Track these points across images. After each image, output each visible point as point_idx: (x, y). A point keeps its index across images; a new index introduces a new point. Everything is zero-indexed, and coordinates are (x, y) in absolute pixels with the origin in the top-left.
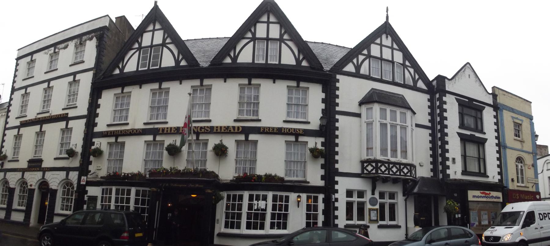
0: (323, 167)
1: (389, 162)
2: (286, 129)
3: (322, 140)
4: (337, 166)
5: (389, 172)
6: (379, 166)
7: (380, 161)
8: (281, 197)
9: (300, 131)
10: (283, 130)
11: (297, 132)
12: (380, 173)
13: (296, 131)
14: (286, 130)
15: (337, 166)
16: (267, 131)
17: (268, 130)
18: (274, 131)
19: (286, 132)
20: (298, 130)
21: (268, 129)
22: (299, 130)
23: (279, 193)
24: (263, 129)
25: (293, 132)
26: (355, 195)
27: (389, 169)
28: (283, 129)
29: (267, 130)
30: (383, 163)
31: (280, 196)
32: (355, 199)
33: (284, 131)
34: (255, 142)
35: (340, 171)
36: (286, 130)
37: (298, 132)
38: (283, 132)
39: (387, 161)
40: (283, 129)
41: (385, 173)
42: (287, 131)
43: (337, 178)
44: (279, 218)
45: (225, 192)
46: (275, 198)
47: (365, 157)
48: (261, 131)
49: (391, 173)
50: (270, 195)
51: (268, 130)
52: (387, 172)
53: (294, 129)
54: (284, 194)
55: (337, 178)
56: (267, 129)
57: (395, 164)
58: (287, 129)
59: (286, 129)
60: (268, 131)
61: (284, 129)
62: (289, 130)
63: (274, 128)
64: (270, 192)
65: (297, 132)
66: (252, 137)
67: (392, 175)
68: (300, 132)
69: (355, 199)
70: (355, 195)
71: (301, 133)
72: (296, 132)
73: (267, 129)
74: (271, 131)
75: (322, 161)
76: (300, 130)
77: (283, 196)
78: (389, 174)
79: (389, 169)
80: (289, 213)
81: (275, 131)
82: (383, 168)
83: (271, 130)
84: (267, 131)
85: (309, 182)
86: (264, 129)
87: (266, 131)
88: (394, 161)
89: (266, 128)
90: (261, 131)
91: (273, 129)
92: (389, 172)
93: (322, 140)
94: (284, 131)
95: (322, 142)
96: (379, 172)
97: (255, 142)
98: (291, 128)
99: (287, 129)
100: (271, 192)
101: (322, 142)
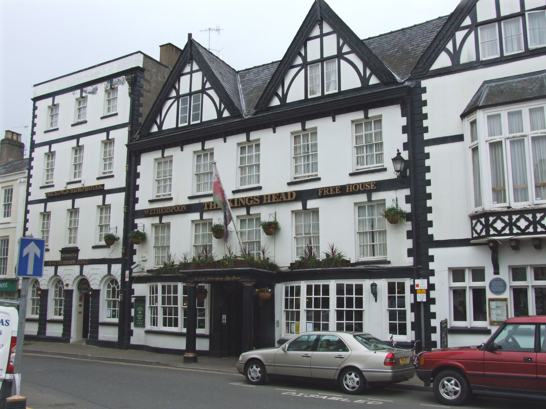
0: (409, 235)
1: (510, 212)
2: (351, 186)
3: (407, 192)
4: (430, 231)
5: (511, 230)
6: (490, 222)
7: (492, 214)
8: (349, 287)
9: (370, 185)
10: (347, 188)
11: (366, 189)
12: (494, 235)
13: (365, 186)
14: (351, 188)
15: (430, 231)
16: (326, 193)
17: (328, 192)
18: (335, 192)
19: (351, 191)
20: (368, 184)
21: (328, 190)
22: (369, 183)
23: (346, 282)
24: (321, 192)
25: (361, 189)
26: (468, 276)
27: (511, 224)
28: (347, 186)
29: (327, 192)
30: (498, 215)
31: (347, 285)
32: (468, 283)
33: (349, 190)
34: (316, 211)
35: (436, 238)
36: (351, 188)
37: (368, 188)
38: (347, 191)
39: (505, 209)
40: (347, 186)
41: (503, 233)
42: (352, 190)
43: (432, 252)
44: (349, 318)
45: (282, 283)
46: (340, 290)
47: (473, 209)
48: (320, 194)
49: (515, 231)
50: (333, 284)
51: (328, 192)
52: (507, 231)
53: (362, 184)
54: (354, 282)
55: (432, 252)
56: (326, 190)
57: (522, 213)
58: (352, 186)
59: (351, 186)
60: (328, 193)
61: (349, 187)
62: (356, 187)
63: (335, 187)
64: (332, 280)
65: (366, 189)
66: (311, 204)
67: (517, 234)
68: (370, 188)
69: (468, 283)
70: (468, 276)
71: (372, 188)
72: (365, 188)
73: (326, 190)
74: (331, 193)
75: (408, 226)
76: (370, 184)
77: (353, 285)
78: (511, 233)
79: (511, 224)
80: (364, 310)
81: (337, 192)
82: (499, 225)
83: (331, 190)
84: (326, 193)
85: (389, 262)
86: (323, 192)
87: (325, 194)
88: (523, 207)
89: (325, 189)
90: (320, 194)
91: (334, 188)
92: (511, 230)
93: (407, 192)
94: (349, 190)
95: (407, 197)
96: (492, 232)
97: (316, 211)
98: (358, 184)
99: (352, 186)
100: (334, 280)
101: (407, 197)
